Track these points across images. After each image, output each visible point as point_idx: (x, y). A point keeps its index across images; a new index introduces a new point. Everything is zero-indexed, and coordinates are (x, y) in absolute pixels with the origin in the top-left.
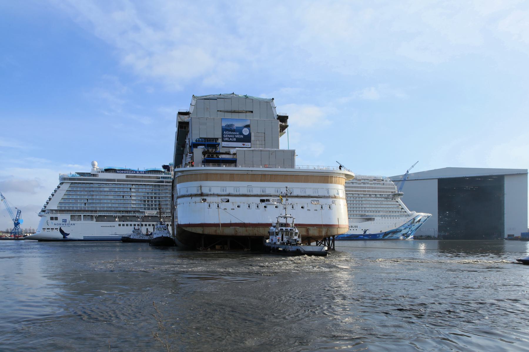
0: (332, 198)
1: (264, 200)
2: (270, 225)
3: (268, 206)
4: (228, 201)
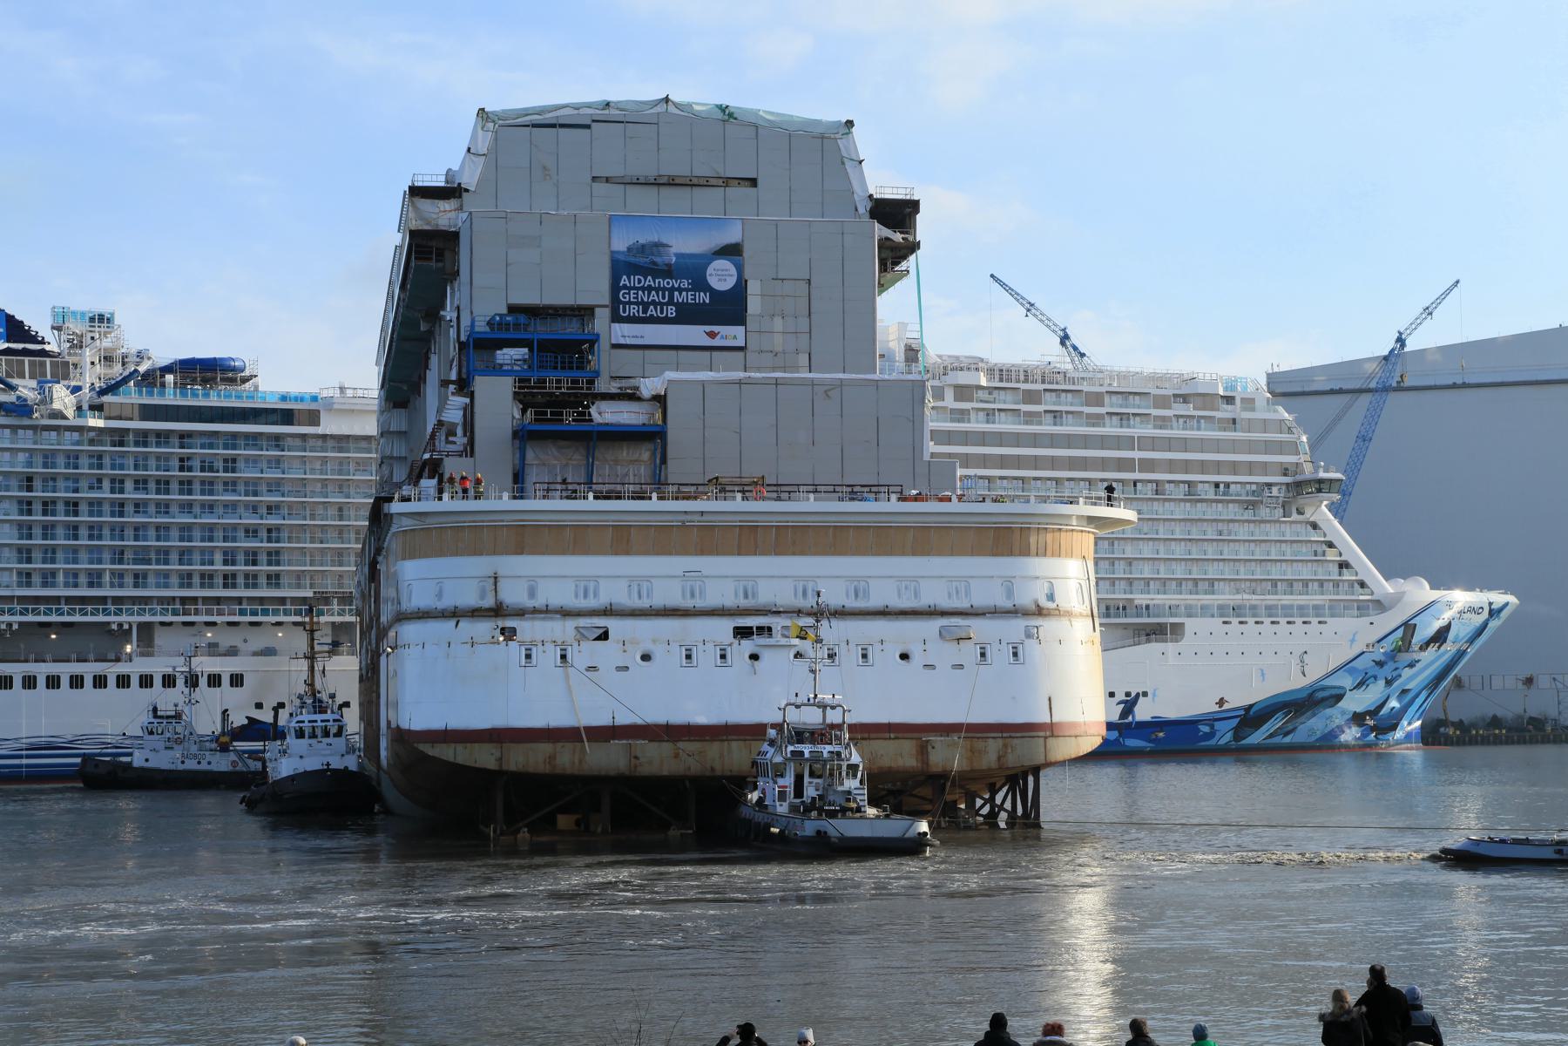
0: (1026, 613)
1: (750, 628)
2: (755, 731)
3: (766, 655)
4: (604, 636)
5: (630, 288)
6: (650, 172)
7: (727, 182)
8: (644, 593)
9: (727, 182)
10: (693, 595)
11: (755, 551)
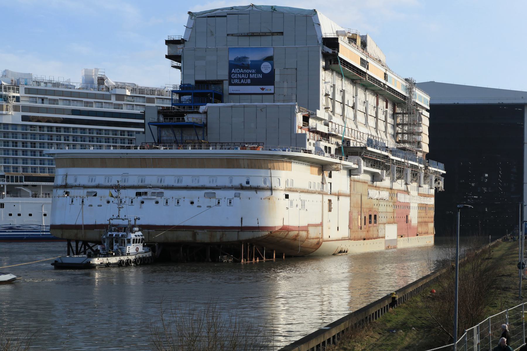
5: (235, 73)
6: (246, 31)
7: (273, 34)
8: (110, 181)
9: (273, 34)
10: (125, 181)
11: (146, 166)
